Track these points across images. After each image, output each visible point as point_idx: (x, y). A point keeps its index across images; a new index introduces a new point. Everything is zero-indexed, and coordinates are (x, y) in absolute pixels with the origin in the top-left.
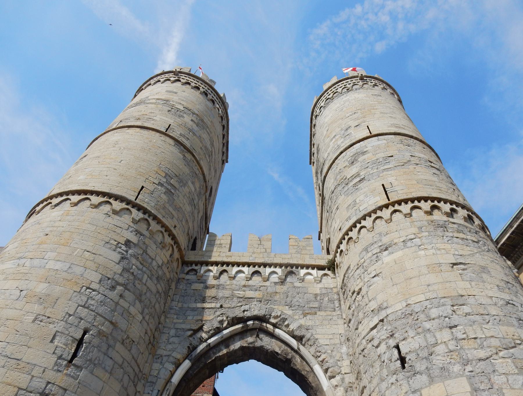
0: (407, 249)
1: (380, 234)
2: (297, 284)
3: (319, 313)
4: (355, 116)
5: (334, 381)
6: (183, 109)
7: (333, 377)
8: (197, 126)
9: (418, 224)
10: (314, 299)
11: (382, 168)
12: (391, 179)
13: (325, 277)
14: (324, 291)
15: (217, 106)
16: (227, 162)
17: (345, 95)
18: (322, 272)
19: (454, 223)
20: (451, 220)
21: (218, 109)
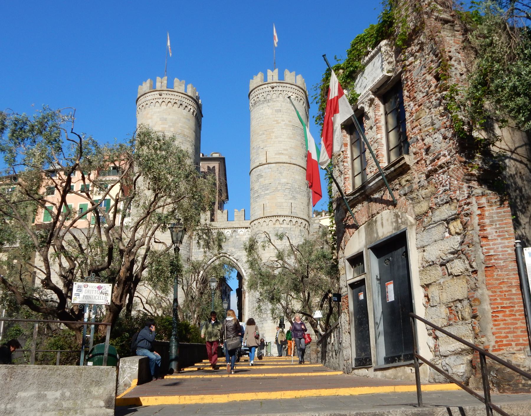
2: (237, 237)
18: (247, 230)
20: (282, 226)
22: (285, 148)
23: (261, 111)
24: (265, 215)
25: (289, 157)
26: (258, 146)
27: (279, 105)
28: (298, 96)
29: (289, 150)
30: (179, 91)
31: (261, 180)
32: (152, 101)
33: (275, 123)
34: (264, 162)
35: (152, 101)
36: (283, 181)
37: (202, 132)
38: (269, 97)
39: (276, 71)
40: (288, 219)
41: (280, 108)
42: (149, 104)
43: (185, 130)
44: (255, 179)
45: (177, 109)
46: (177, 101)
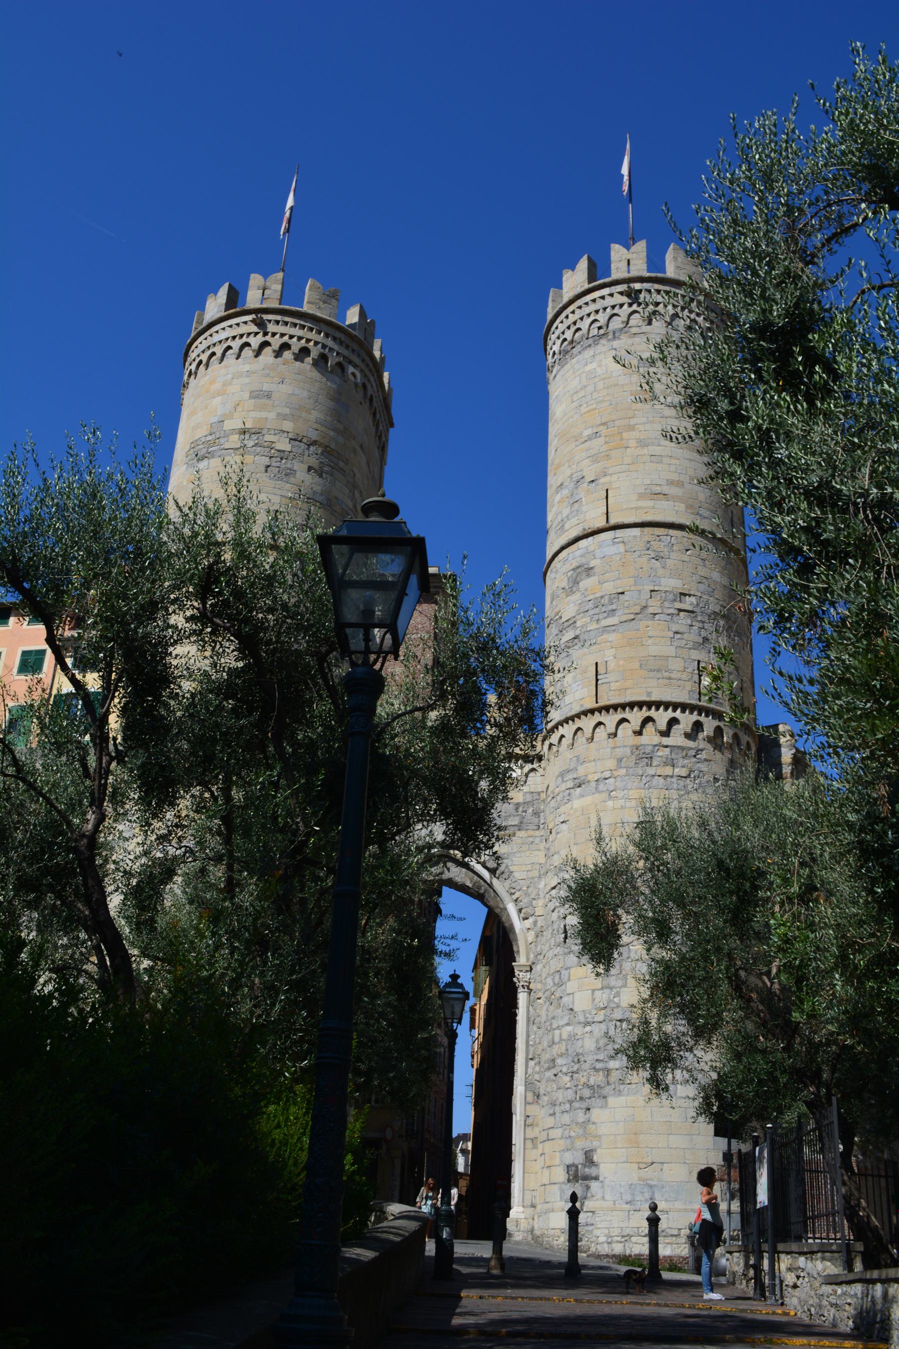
0: (597, 795)
1: (578, 757)
3: (518, 834)
4: (597, 444)
5: (528, 923)
6: (288, 447)
7: (525, 919)
8: (321, 476)
9: (619, 752)
10: (514, 812)
11: (605, 623)
12: (609, 654)
13: (532, 774)
14: (529, 798)
15: (351, 369)
16: (392, 425)
18: (528, 767)
19: (666, 747)
20: (665, 741)
21: (353, 374)
22: (675, 477)
23: (590, 367)
24: (602, 702)
25: (689, 507)
26: (576, 477)
30: (319, 314)
31: (586, 583)
34: (601, 523)
35: (229, 343)
36: (671, 584)
37: (387, 468)
38: (616, 323)
39: (641, 247)
40: (687, 720)
44: (564, 584)
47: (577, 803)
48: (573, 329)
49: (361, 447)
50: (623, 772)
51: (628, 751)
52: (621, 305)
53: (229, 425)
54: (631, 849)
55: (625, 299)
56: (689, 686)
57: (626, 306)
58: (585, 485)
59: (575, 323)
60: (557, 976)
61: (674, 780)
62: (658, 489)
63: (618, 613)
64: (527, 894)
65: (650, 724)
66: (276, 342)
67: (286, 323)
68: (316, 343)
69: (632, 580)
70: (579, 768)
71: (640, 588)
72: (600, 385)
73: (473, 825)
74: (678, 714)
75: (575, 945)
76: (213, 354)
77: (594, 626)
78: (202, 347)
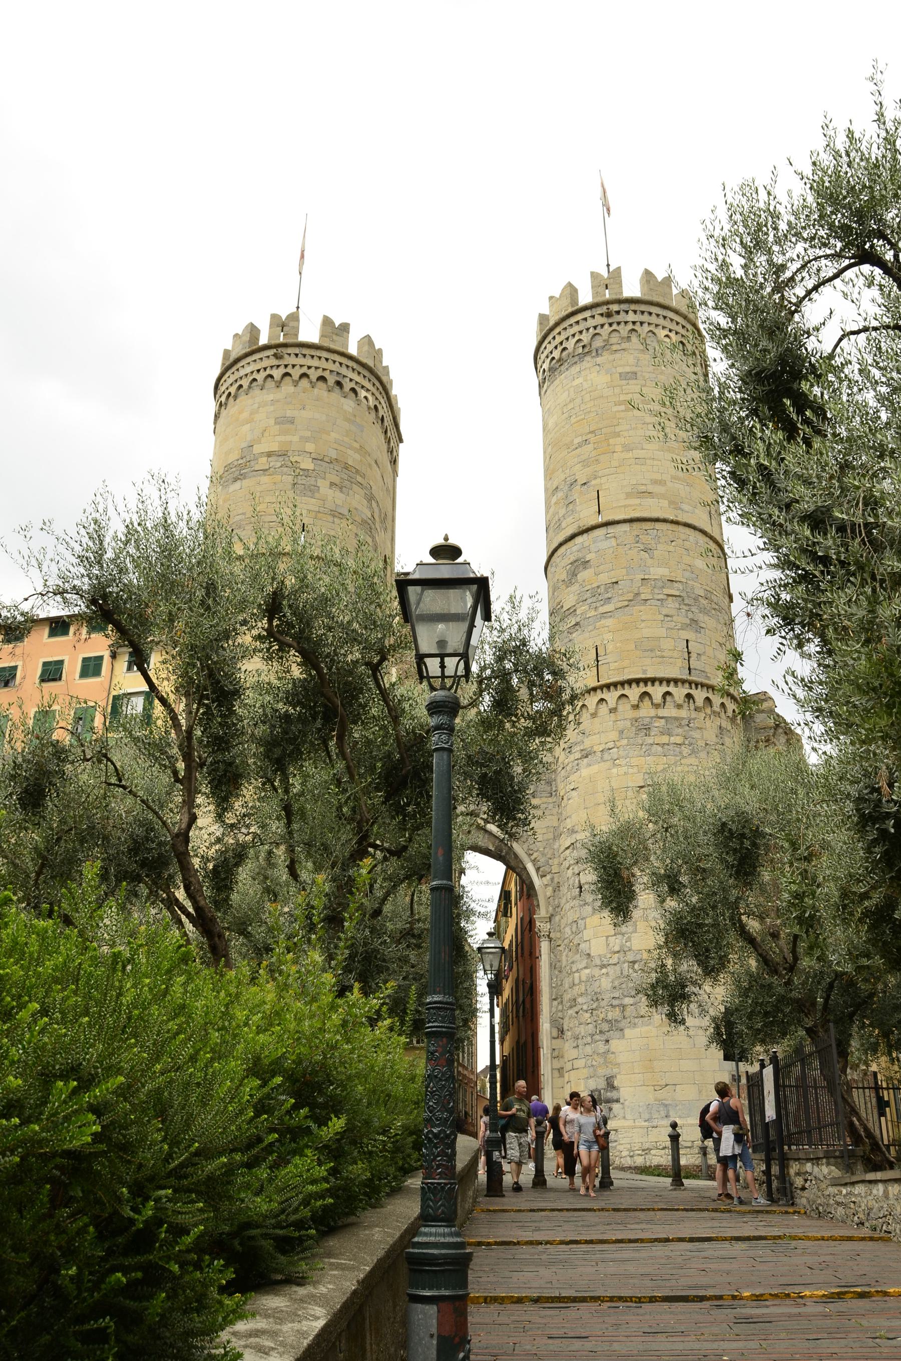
15: (363, 393)
17: (576, 368)
20: (662, 712)
22: (658, 477)
23: (577, 382)
24: (602, 682)
27: (631, 360)
28: (685, 342)
29: (669, 484)
30: (332, 346)
31: (583, 575)
32: (255, 376)
33: (623, 407)
36: (659, 572)
38: (598, 343)
40: (679, 692)
41: (634, 369)
42: (245, 386)
43: (350, 452)
44: (564, 576)
45: (326, 394)
46: (326, 374)
47: (585, 772)
48: (560, 348)
49: (376, 462)
50: (625, 742)
51: (628, 723)
52: (602, 326)
53: (257, 449)
54: (641, 814)
55: (604, 320)
56: (679, 663)
57: (606, 326)
58: (578, 487)
59: (561, 343)
60: (575, 925)
61: (671, 747)
62: (643, 488)
63: (614, 601)
64: (543, 854)
65: (647, 698)
66: (296, 373)
67: (304, 356)
68: (331, 371)
69: (624, 571)
70: (586, 740)
71: (632, 577)
72: (587, 398)
73: (507, 802)
74: (671, 688)
75: (593, 899)
76: (241, 386)
77: (593, 613)
78: (230, 381)
